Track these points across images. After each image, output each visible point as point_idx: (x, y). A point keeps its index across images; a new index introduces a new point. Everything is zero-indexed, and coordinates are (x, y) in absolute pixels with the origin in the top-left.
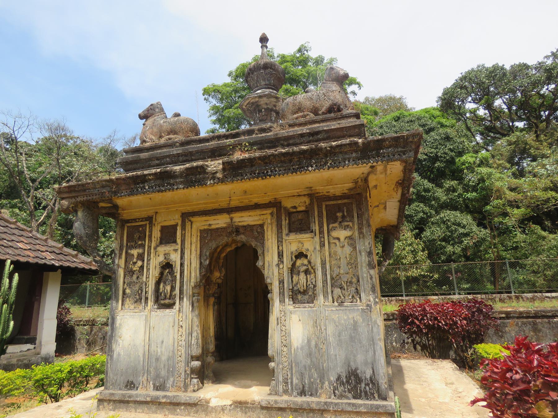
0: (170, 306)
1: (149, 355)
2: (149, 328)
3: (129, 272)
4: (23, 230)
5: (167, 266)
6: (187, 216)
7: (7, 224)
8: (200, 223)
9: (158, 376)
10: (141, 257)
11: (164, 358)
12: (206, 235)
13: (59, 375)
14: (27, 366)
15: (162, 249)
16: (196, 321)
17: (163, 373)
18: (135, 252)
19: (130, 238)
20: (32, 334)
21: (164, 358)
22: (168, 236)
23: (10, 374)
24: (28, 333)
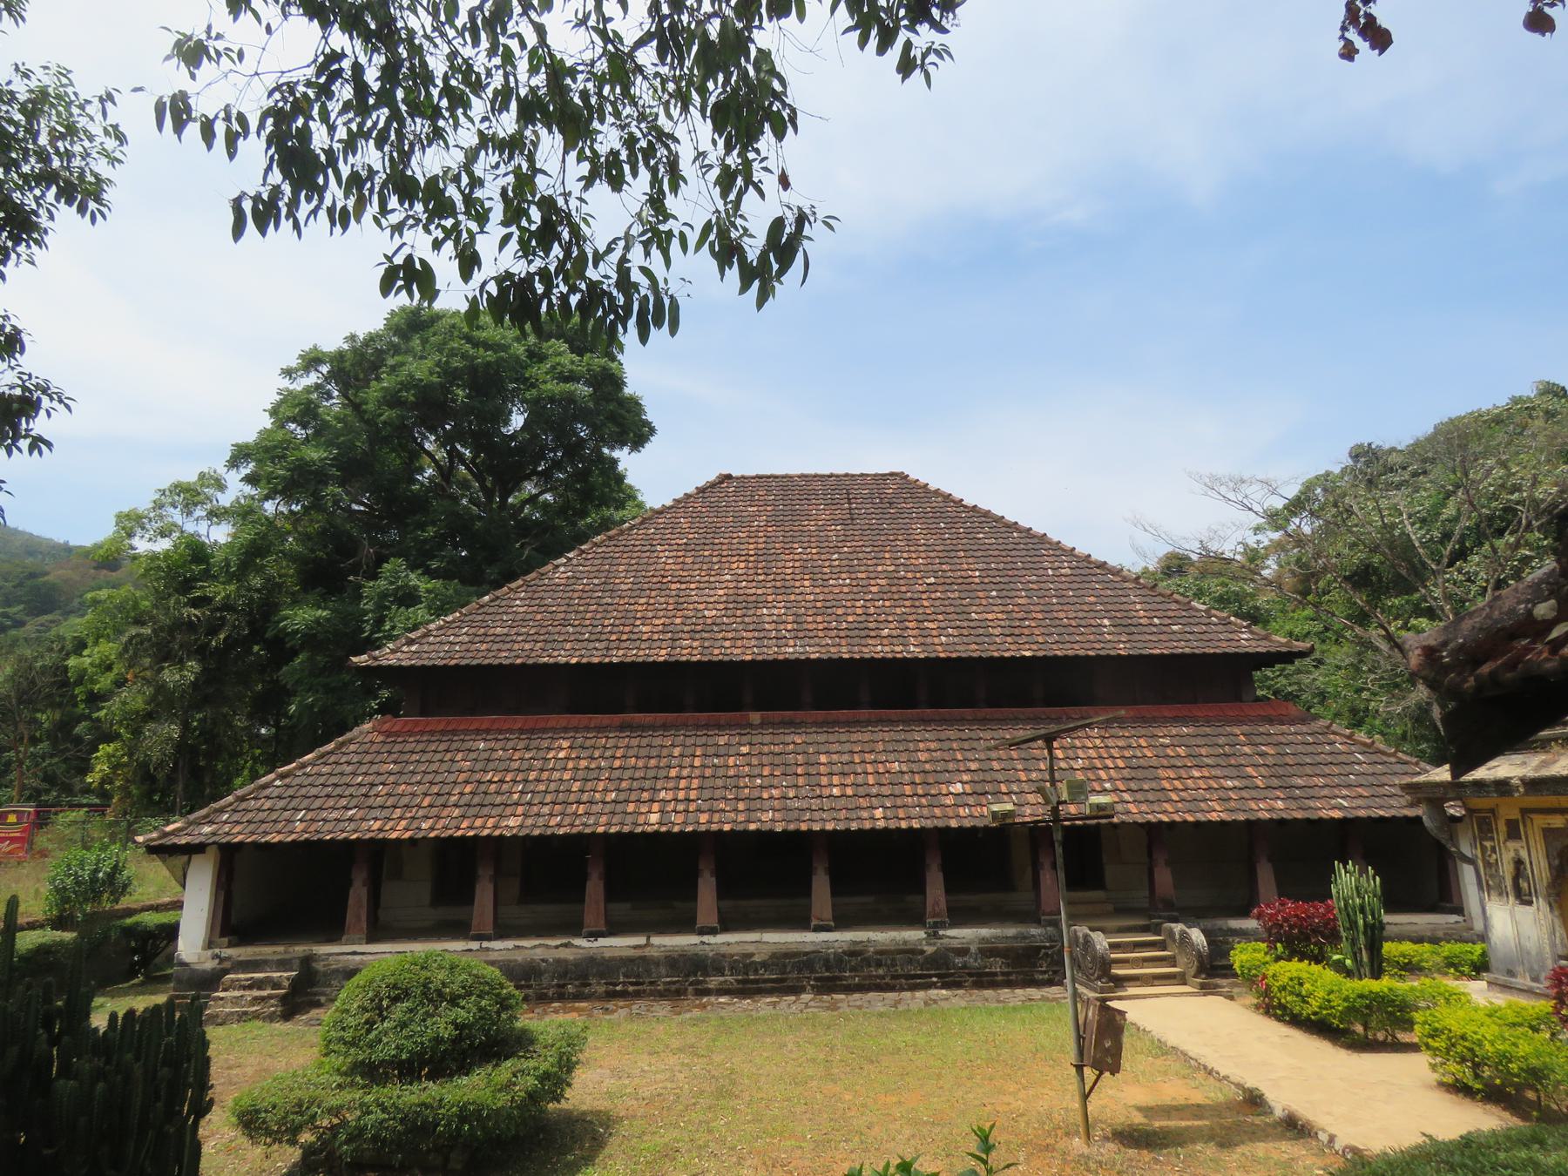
0: (1530, 903)
1: (1519, 945)
2: (1516, 923)
3: (1487, 865)
4: (1406, 763)
5: (1518, 863)
6: (1525, 812)
7: (1385, 758)
8: (1540, 821)
9: (1531, 970)
10: (1493, 850)
11: (1534, 953)
12: (1548, 833)
13: (1469, 956)
14: (1434, 941)
15: (1511, 845)
16: (1557, 922)
17: (1536, 967)
18: (1488, 844)
19: (1480, 829)
20: (1455, 899)
21: (1534, 953)
22: (1513, 832)
23: (1416, 947)
24: (1450, 900)
